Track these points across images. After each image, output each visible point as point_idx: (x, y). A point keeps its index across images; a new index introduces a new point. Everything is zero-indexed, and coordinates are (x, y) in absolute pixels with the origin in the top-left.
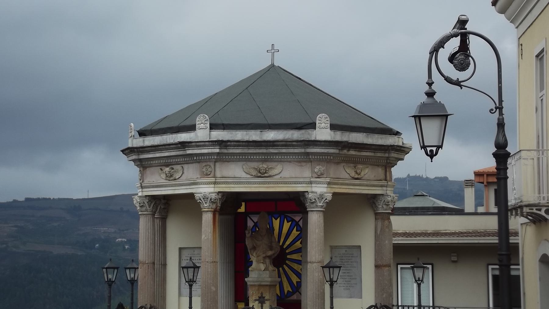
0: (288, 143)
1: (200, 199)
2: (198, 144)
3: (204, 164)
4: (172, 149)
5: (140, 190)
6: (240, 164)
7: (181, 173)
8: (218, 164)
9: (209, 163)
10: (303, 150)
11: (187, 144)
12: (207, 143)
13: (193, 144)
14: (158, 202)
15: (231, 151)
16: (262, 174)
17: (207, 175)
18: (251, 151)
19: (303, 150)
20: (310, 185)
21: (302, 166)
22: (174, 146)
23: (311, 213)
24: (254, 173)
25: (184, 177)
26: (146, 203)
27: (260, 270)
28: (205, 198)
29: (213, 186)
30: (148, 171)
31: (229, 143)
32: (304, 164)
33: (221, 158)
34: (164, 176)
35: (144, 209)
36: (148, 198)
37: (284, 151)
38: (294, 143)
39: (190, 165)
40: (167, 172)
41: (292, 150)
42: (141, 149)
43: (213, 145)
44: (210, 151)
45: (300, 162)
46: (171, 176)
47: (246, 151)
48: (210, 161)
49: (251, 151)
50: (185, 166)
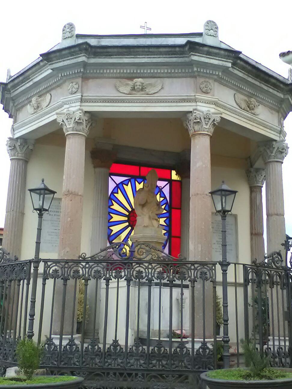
0: (278, 84)
1: (200, 119)
2: (211, 50)
3: (202, 80)
4: (161, 53)
5: (79, 104)
6: (233, 92)
7: (160, 88)
8: (216, 84)
9: (207, 80)
10: (282, 96)
11: (197, 47)
12: (222, 52)
13: (206, 49)
14: (93, 125)
15: (236, 72)
16: (250, 108)
17: (206, 93)
18: (250, 79)
19: (282, 96)
20: (279, 135)
21: (272, 113)
22: (167, 49)
23: (276, 163)
24: (244, 105)
25: (162, 93)
26: (84, 120)
27: (153, 226)
28: (207, 118)
29: (214, 106)
30: (91, 83)
31: (239, 61)
32: (274, 112)
33: (224, 78)
34: (127, 90)
35: (81, 127)
36: (87, 115)
37: (271, 90)
38: (282, 85)
39: (175, 80)
40: (138, 84)
41: (275, 93)
42: (98, 50)
43: (228, 57)
44: (220, 63)
45: (271, 108)
46: (142, 89)
47: (245, 77)
48: (209, 78)
49: (250, 79)
50: (167, 81)
